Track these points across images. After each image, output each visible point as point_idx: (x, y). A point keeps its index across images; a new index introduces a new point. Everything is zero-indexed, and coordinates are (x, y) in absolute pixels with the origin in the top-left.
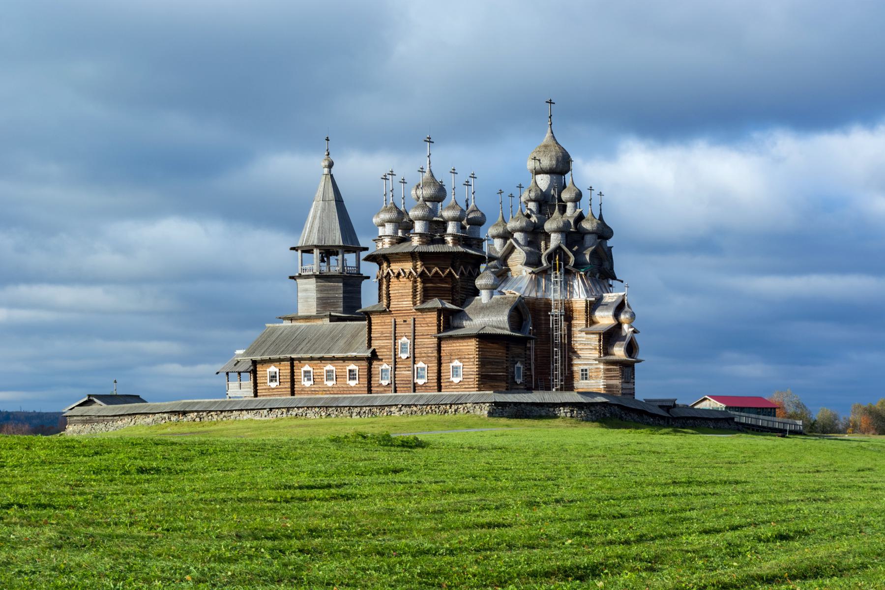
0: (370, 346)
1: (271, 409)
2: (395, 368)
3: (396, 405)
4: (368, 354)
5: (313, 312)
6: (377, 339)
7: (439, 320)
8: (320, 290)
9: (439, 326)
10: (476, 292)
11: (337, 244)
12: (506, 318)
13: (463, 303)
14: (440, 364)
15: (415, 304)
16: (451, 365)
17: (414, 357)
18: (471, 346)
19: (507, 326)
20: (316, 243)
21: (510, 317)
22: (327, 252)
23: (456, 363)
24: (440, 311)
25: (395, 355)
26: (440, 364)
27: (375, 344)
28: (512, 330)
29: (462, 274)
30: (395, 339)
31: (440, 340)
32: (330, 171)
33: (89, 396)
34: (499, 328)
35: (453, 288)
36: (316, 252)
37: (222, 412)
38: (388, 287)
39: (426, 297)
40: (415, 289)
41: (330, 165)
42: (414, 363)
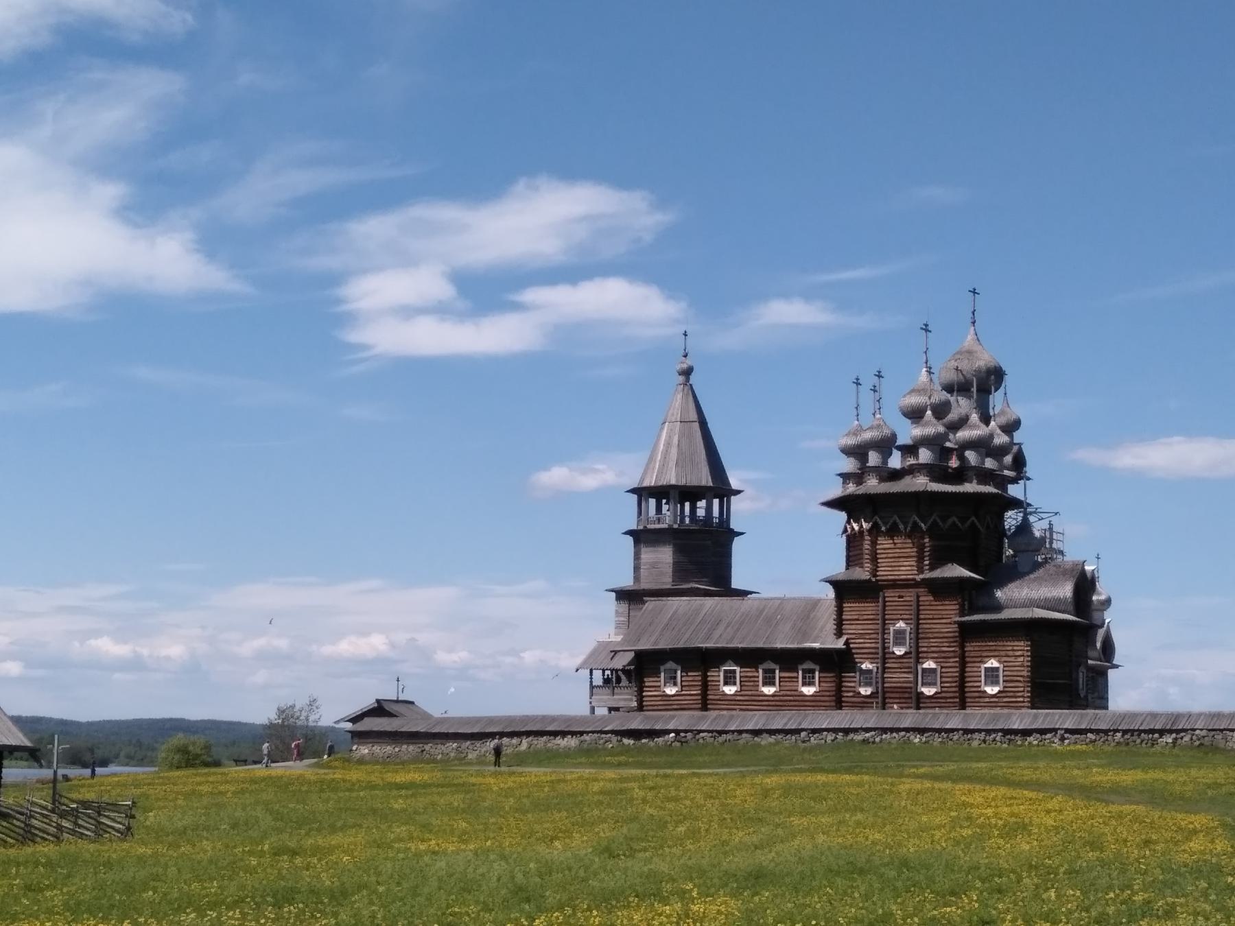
0: (839, 633)
1: (814, 731)
2: (884, 668)
3: (1055, 730)
5: (667, 582)
8: (678, 550)
9: (962, 606)
11: (704, 483)
14: (963, 664)
15: (921, 571)
17: (918, 653)
19: (1071, 608)
20: (673, 482)
22: (689, 494)
24: (962, 581)
25: (884, 648)
26: (963, 664)
29: (988, 527)
30: (884, 624)
32: (688, 380)
33: (378, 701)
37: (720, 733)
38: (874, 543)
41: (687, 373)
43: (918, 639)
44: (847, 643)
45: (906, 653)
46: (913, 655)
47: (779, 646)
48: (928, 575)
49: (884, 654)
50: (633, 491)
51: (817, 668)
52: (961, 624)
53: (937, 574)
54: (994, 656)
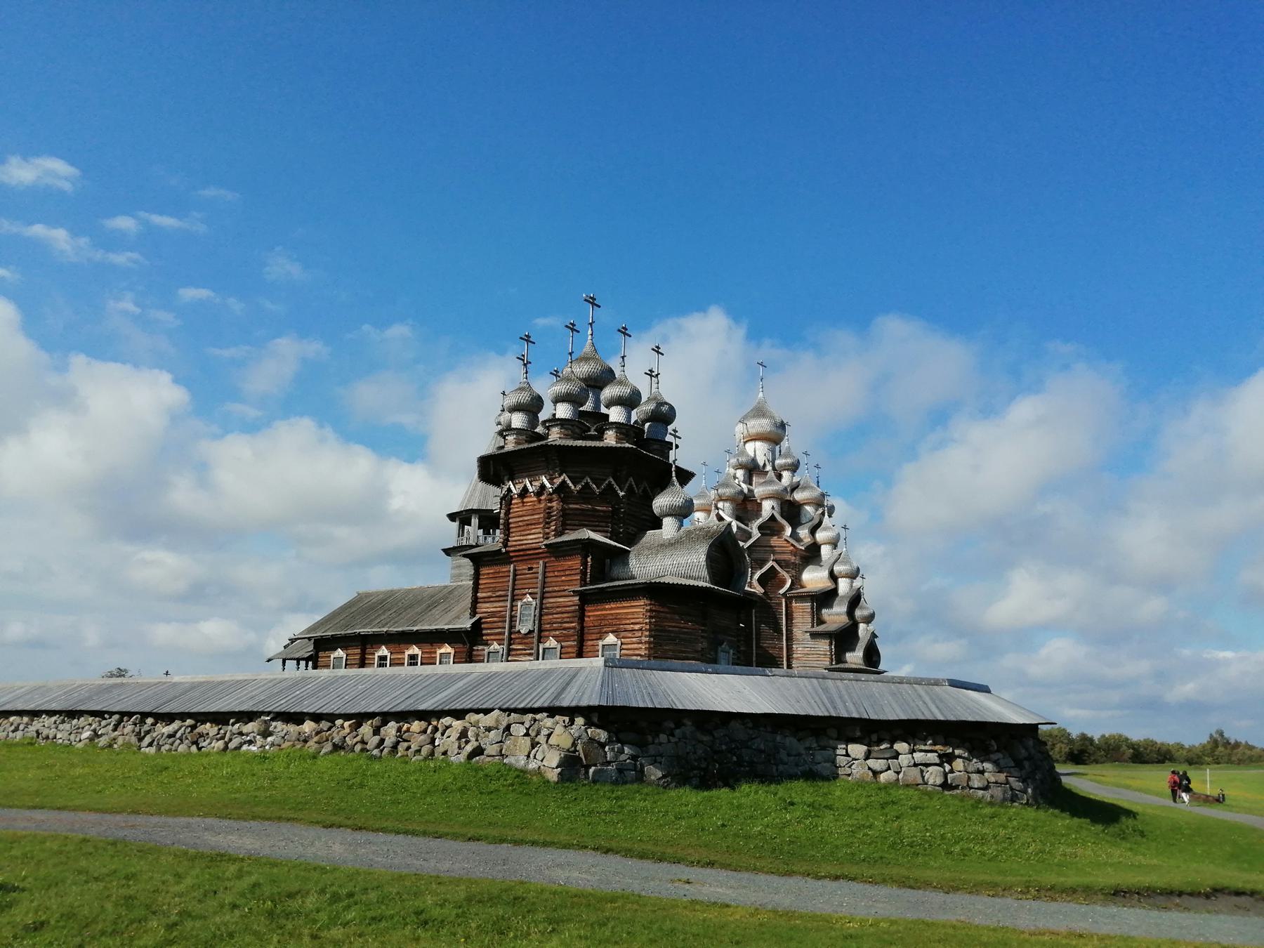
0: (473, 613)
2: (509, 650)
4: (466, 624)
6: (487, 600)
7: (585, 564)
9: (584, 573)
10: (657, 524)
12: (703, 558)
13: (632, 539)
16: (601, 643)
17: (540, 630)
18: (638, 610)
19: (705, 573)
21: (710, 558)
23: (611, 639)
25: (512, 627)
27: (484, 608)
28: (714, 577)
29: (630, 491)
30: (513, 600)
31: (586, 599)
34: (690, 577)
35: (615, 512)
36: (475, 521)
39: (568, 520)
40: (549, 515)
42: (539, 642)
43: (541, 615)
44: (477, 626)
45: (530, 632)
46: (535, 634)
47: (415, 629)
48: (553, 540)
49: (510, 633)
50: (452, 517)
51: (452, 651)
52: (582, 595)
53: (559, 540)
54: (612, 632)
